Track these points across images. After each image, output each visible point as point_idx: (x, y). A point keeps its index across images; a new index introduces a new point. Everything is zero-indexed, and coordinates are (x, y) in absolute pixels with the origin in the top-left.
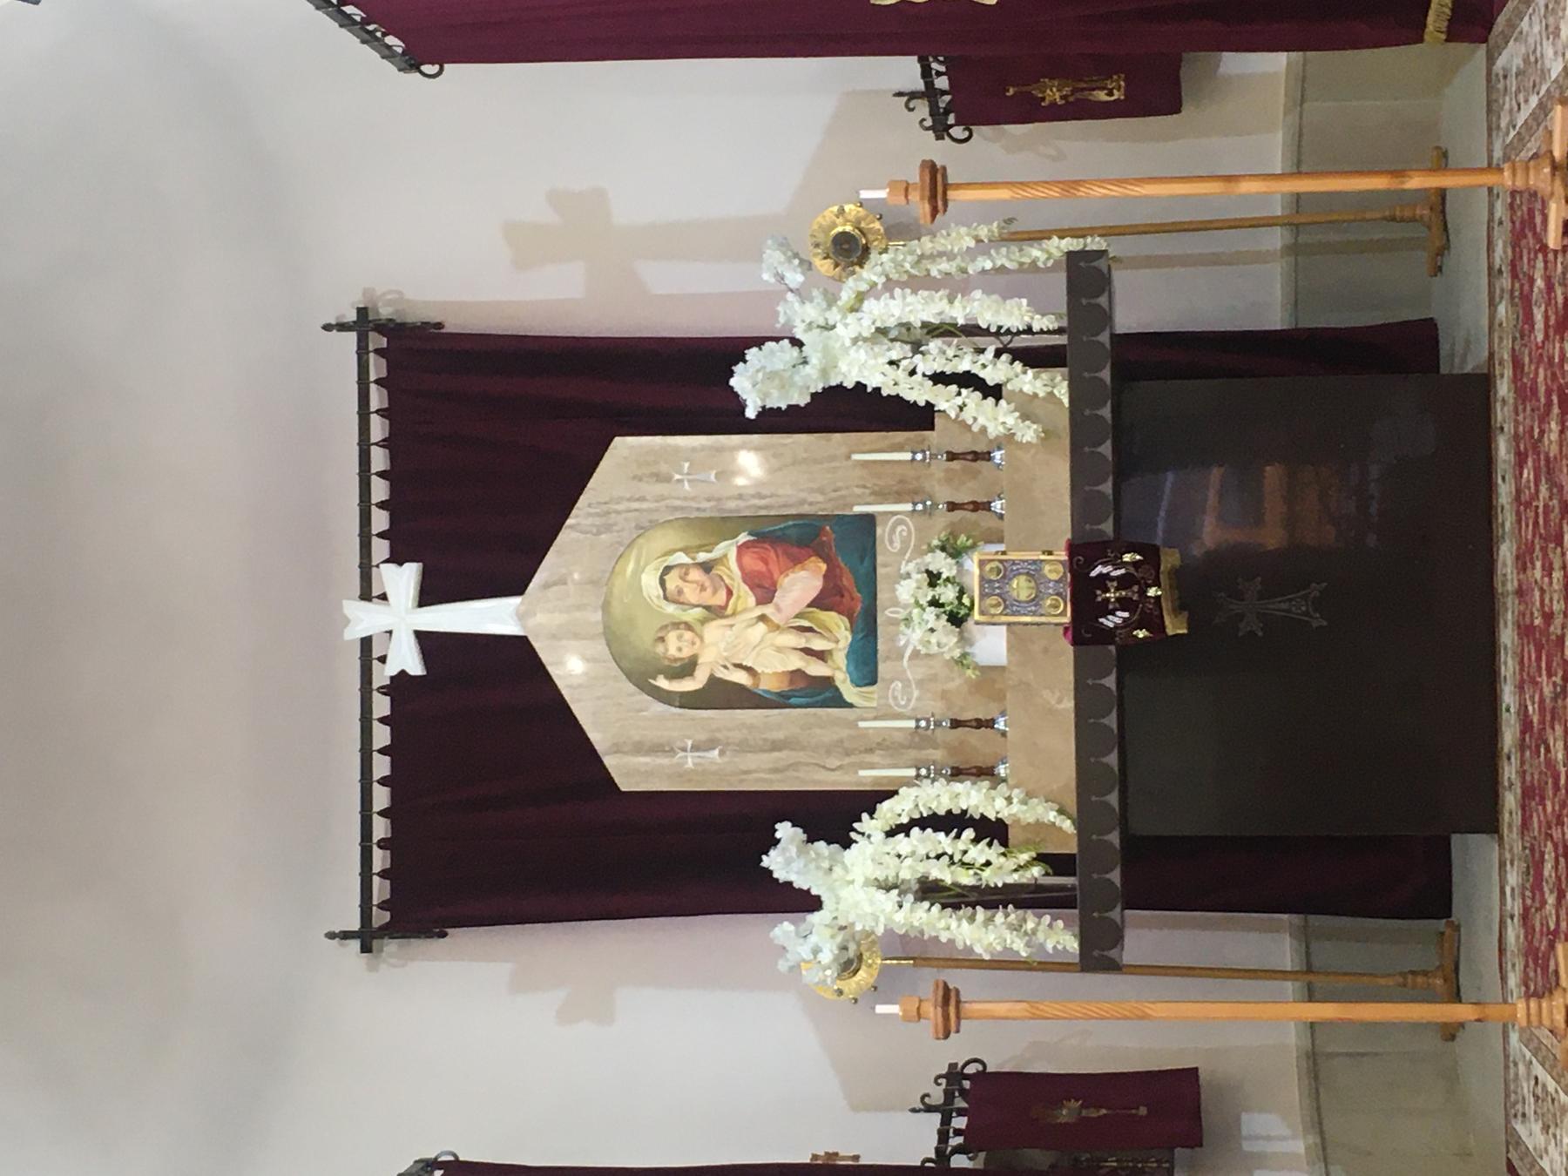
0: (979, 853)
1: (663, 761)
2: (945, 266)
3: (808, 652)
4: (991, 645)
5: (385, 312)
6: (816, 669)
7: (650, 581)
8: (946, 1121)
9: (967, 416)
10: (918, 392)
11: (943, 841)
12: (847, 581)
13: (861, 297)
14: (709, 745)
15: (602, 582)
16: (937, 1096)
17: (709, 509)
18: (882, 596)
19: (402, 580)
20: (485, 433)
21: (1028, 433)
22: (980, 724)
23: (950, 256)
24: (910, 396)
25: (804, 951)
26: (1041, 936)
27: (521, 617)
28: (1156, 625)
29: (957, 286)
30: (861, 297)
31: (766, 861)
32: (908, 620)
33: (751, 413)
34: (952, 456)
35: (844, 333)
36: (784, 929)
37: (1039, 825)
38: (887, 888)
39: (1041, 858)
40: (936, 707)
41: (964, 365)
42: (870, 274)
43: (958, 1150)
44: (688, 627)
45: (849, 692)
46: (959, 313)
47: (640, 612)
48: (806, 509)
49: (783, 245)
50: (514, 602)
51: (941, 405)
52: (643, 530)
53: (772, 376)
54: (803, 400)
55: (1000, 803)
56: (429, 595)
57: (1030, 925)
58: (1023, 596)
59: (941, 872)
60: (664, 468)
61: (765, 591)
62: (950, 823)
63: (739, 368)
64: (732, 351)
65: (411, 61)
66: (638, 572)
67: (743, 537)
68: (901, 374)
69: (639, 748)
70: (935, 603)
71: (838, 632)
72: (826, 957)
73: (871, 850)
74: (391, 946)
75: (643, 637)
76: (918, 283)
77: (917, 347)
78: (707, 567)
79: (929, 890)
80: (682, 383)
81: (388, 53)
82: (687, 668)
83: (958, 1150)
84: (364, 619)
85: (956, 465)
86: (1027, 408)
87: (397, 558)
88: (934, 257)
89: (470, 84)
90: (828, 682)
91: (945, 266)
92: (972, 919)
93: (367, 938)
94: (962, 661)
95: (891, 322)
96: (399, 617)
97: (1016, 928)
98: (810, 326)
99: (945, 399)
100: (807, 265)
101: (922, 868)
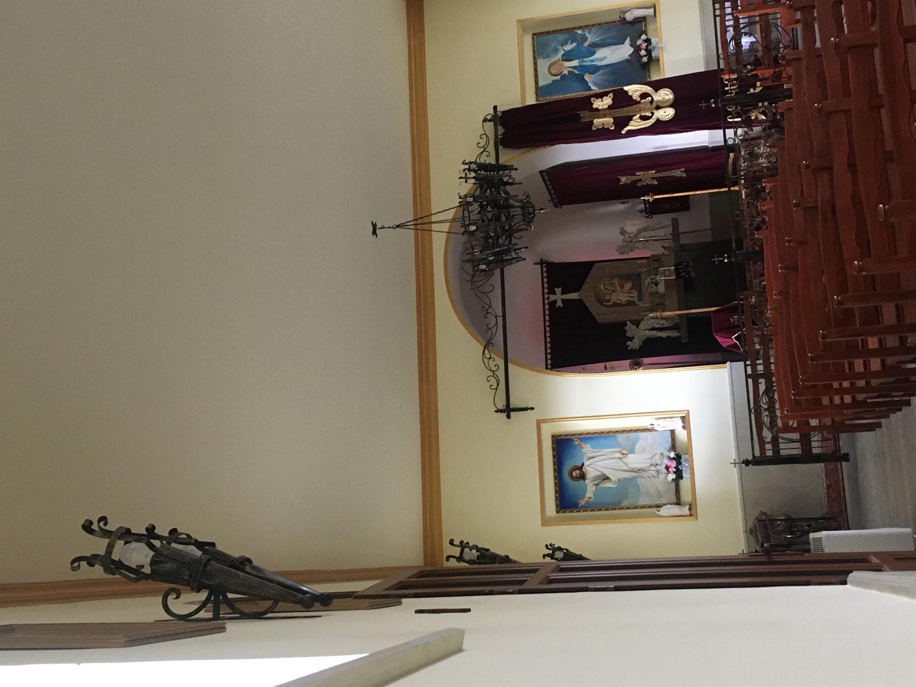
19: (558, 290)
28: (690, 275)
45: (637, 303)
56: (563, 293)
61: (622, 287)
71: (635, 294)
79: (653, 329)
82: (609, 301)
84: (552, 298)
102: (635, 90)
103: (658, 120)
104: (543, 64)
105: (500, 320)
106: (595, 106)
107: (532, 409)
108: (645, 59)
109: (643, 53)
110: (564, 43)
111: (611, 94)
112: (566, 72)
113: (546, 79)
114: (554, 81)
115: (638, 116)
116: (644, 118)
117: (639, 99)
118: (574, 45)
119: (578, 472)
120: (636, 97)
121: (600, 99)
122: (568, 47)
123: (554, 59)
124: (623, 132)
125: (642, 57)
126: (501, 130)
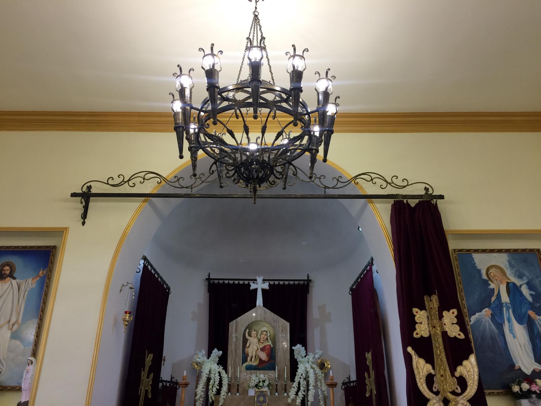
0: (215, 390)
1: (234, 331)
2: (319, 385)
3: (252, 357)
4: (252, 392)
5: (311, 284)
6: (249, 359)
7: (265, 329)
8: (169, 382)
9: (293, 389)
10: (297, 379)
11: (217, 383)
12: (264, 365)
13: (313, 368)
14: (236, 339)
15: (265, 320)
16: (174, 380)
17: (277, 340)
18: (261, 371)
19: (266, 286)
20: (291, 301)
21: (289, 401)
22: (238, 390)
23: (321, 386)
24: (296, 378)
25: (200, 356)
26: (199, 401)
27: (259, 306)
29: (316, 387)
30: (313, 368)
31: (216, 349)
32: (257, 376)
33: (293, 348)
34: (286, 385)
35: (307, 365)
36: (204, 352)
37: (219, 401)
38: (210, 372)
39: (213, 402)
40: (241, 382)
41: (302, 388)
42: (318, 370)
43: (163, 384)
44: (257, 335)
45: (245, 365)
46: (311, 387)
47: (260, 327)
48: (277, 357)
49: (322, 354)
50: (262, 305)
51: (294, 384)
52: (274, 327)
53: (300, 351)
54: (296, 357)
55: (223, 394)
56: (263, 290)
57: (201, 399)
58: (260, 399)
59: (212, 382)
60: (284, 332)
61: (263, 349)
62: (220, 384)
63: (301, 346)
64: (304, 344)
65: (351, 289)
66: (266, 326)
67: (272, 346)
68: (300, 376)
69: (236, 326)
70: (260, 381)
71: (255, 363)
72: (198, 360)
73: (216, 368)
74: (207, 283)
75: (255, 327)
76: (316, 380)
77: (305, 379)
78: (267, 339)
79: (209, 379)
80: (299, 336)
81: (353, 286)
82: (250, 335)
83: (163, 384)
84: (260, 280)
85: (284, 386)
86: (294, 400)
87: (270, 285)
88: (321, 383)
89: (349, 299)
90: (246, 361)
91: (319, 385)
92: (203, 388)
93: (209, 279)
94: (249, 387)
95: (309, 374)
96: (260, 285)
97: (201, 396)
98: (308, 359)
99: (295, 384)
100: (319, 358)
101: (213, 378)
102: (470, 368)
103: (428, 400)
104: (502, 260)
105: (188, 191)
106: (445, 313)
107: (83, 223)
108: (516, 389)
109: (525, 386)
110: (530, 286)
111: (462, 336)
112: (492, 286)
113: (481, 262)
114: (479, 271)
115: (432, 372)
116: (430, 380)
117: (457, 374)
118: (530, 299)
119: (8, 272)
120: (460, 370)
121: (455, 321)
122: (525, 291)
123: (508, 272)
124: (409, 349)
125: (519, 384)
126: (413, 203)
